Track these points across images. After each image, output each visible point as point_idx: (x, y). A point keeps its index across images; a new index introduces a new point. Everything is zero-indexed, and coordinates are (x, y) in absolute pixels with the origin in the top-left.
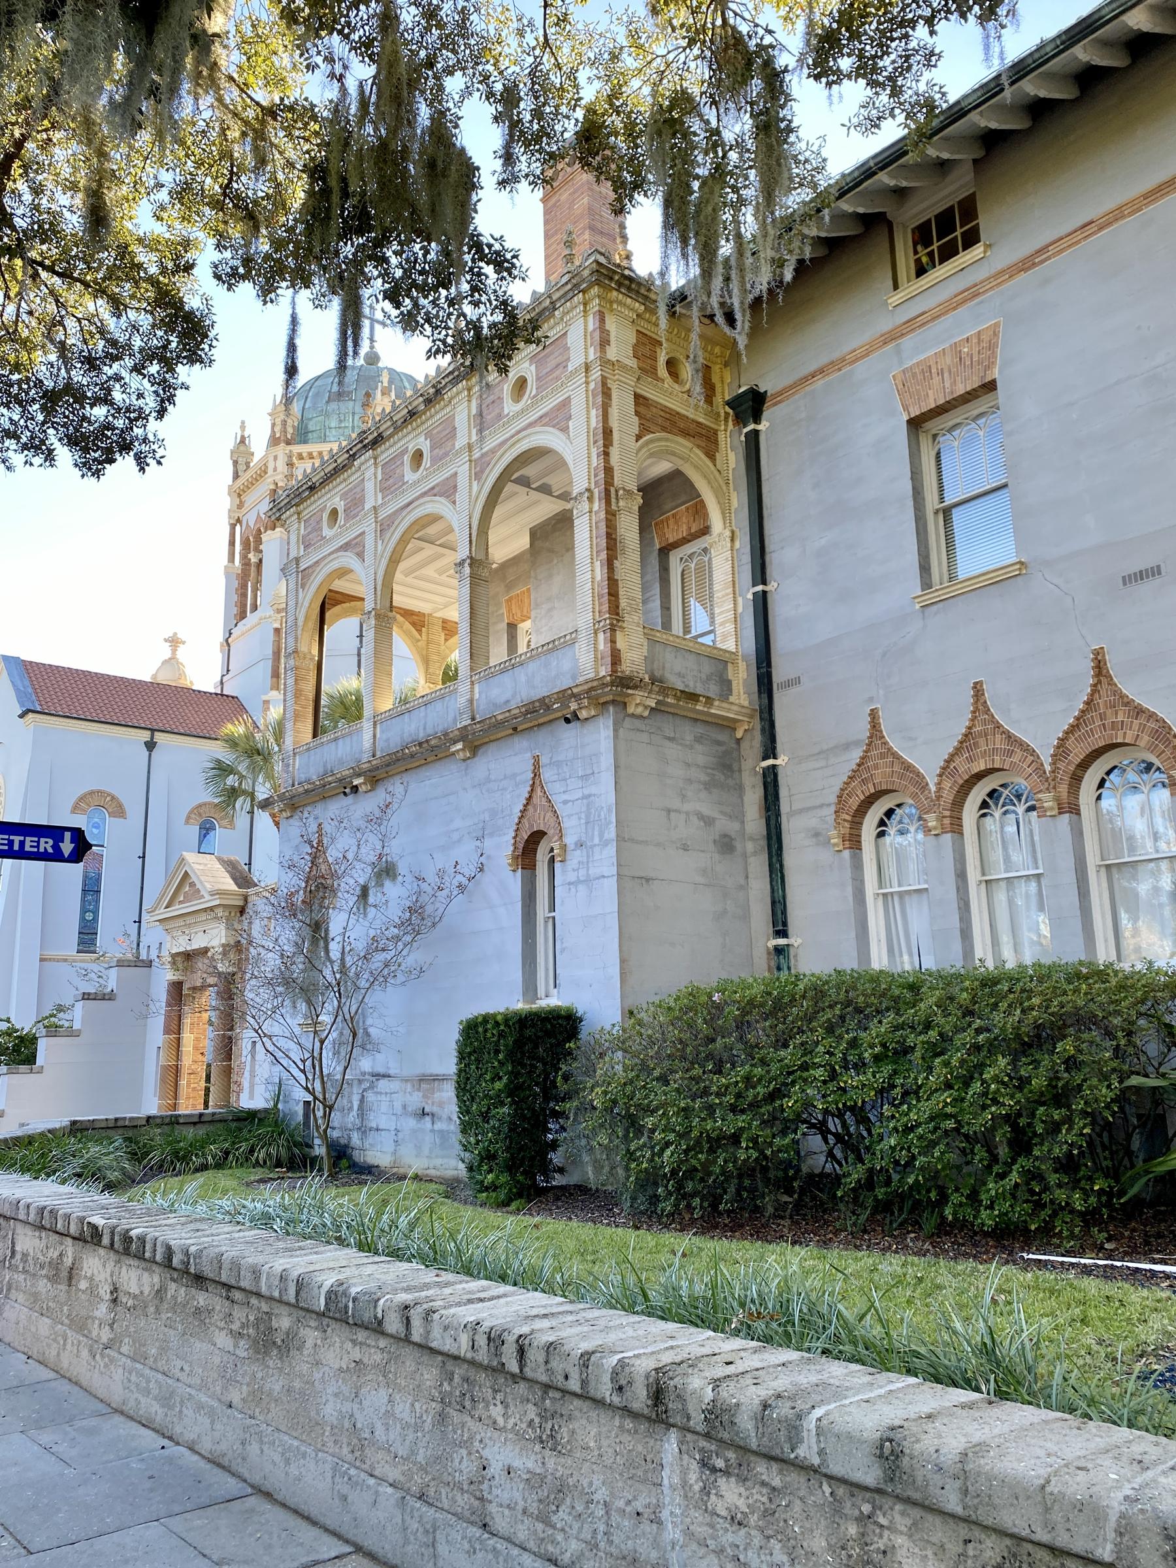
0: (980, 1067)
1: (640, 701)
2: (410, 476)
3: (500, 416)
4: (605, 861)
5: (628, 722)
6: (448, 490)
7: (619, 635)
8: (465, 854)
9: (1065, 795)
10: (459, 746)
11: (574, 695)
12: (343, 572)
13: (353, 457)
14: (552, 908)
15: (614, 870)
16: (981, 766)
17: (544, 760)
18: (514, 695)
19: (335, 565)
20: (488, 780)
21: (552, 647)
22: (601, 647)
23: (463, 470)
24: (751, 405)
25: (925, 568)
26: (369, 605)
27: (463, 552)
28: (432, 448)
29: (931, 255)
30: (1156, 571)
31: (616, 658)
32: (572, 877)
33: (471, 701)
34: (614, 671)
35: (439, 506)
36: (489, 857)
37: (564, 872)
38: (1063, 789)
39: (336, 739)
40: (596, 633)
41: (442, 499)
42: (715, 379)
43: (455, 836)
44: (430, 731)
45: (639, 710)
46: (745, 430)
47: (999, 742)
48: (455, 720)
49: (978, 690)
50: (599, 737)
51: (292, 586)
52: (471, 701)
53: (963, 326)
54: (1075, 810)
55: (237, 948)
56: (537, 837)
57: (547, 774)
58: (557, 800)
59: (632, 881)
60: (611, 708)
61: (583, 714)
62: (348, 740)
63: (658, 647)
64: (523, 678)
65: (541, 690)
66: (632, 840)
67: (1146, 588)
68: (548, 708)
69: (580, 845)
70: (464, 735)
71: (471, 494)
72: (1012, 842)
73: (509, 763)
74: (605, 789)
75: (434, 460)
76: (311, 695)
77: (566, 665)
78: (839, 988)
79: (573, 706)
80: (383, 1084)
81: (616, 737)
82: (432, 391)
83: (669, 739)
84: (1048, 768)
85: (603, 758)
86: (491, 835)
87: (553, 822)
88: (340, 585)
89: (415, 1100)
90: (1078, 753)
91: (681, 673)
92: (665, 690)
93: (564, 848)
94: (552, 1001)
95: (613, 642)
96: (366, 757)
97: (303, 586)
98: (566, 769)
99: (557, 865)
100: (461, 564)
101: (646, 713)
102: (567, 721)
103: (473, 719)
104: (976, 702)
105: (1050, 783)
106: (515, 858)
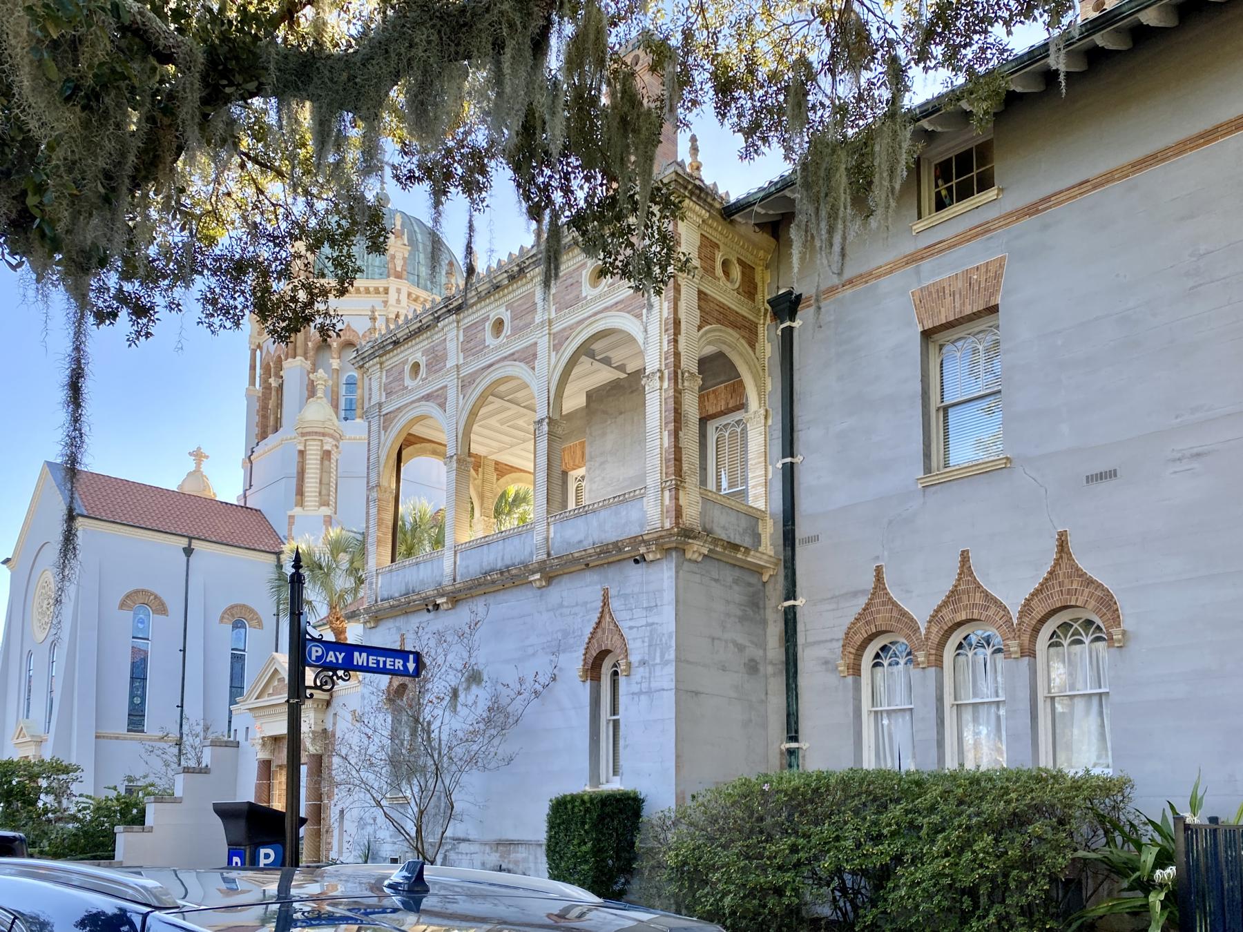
0: (968, 844)
1: (697, 548)
2: (490, 341)
3: (578, 298)
5: (686, 566)
6: (528, 357)
7: (681, 493)
8: (541, 665)
9: (1026, 643)
10: (537, 576)
11: (643, 541)
12: (420, 418)
13: (438, 319)
16: (963, 616)
17: (612, 592)
18: (586, 537)
20: (561, 606)
21: (622, 500)
22: (667, 502)
23: (543, 344)
24: (787, 306)
25: (927, 455)
27: (542, 412)
28: (513, 319)
33: (547, 539)
34: (677, 524)
35: (518, 370)
36: (561, 670)
38: (1026, 638)
40: (662, 490)
41: (522, 364)
42: (758, 279)
43: (530, 651)
44: (508, 562)
45: (696, 556)
46: (782, 326)
47: (978, 598)
48: (531, 554)
49: (965, 557)
50: (663, 577)
51: (374, 428)
52: (547, 539)
54: (1032, 654)
56: (604, 654)
57: (614, 604)
58: (624, 626)
60: (674, 554)
61: (650, 557)
64: (595, 523)
65: (611, 536)
68: (620, 550)
69: (643, 663)
70: (542, 568)
71: (549, 363)
72: (987, 677)
74: (667, 618)
75: (516, 330)
76: (390, 524)
77: (634, 515)
78: (861, 785)
79: (642, 550)
80: (463, 847)
81: (677, 577)
82: (516, 269)
84: (1015, 621)
85: (665, 594)
86: (564, 651)
87: (619, 643)
88: (418, 430)
89: (494, 858)
90: (1039, 610)
95: (677, 499)
96: (447, 581)
97: (385, 429)
98: (632, 601)
100: (540, 422)
102: (636, 561)
103: (549, 554)
104: (962, 566)
105: (1015, 632)
106: (585, 671)
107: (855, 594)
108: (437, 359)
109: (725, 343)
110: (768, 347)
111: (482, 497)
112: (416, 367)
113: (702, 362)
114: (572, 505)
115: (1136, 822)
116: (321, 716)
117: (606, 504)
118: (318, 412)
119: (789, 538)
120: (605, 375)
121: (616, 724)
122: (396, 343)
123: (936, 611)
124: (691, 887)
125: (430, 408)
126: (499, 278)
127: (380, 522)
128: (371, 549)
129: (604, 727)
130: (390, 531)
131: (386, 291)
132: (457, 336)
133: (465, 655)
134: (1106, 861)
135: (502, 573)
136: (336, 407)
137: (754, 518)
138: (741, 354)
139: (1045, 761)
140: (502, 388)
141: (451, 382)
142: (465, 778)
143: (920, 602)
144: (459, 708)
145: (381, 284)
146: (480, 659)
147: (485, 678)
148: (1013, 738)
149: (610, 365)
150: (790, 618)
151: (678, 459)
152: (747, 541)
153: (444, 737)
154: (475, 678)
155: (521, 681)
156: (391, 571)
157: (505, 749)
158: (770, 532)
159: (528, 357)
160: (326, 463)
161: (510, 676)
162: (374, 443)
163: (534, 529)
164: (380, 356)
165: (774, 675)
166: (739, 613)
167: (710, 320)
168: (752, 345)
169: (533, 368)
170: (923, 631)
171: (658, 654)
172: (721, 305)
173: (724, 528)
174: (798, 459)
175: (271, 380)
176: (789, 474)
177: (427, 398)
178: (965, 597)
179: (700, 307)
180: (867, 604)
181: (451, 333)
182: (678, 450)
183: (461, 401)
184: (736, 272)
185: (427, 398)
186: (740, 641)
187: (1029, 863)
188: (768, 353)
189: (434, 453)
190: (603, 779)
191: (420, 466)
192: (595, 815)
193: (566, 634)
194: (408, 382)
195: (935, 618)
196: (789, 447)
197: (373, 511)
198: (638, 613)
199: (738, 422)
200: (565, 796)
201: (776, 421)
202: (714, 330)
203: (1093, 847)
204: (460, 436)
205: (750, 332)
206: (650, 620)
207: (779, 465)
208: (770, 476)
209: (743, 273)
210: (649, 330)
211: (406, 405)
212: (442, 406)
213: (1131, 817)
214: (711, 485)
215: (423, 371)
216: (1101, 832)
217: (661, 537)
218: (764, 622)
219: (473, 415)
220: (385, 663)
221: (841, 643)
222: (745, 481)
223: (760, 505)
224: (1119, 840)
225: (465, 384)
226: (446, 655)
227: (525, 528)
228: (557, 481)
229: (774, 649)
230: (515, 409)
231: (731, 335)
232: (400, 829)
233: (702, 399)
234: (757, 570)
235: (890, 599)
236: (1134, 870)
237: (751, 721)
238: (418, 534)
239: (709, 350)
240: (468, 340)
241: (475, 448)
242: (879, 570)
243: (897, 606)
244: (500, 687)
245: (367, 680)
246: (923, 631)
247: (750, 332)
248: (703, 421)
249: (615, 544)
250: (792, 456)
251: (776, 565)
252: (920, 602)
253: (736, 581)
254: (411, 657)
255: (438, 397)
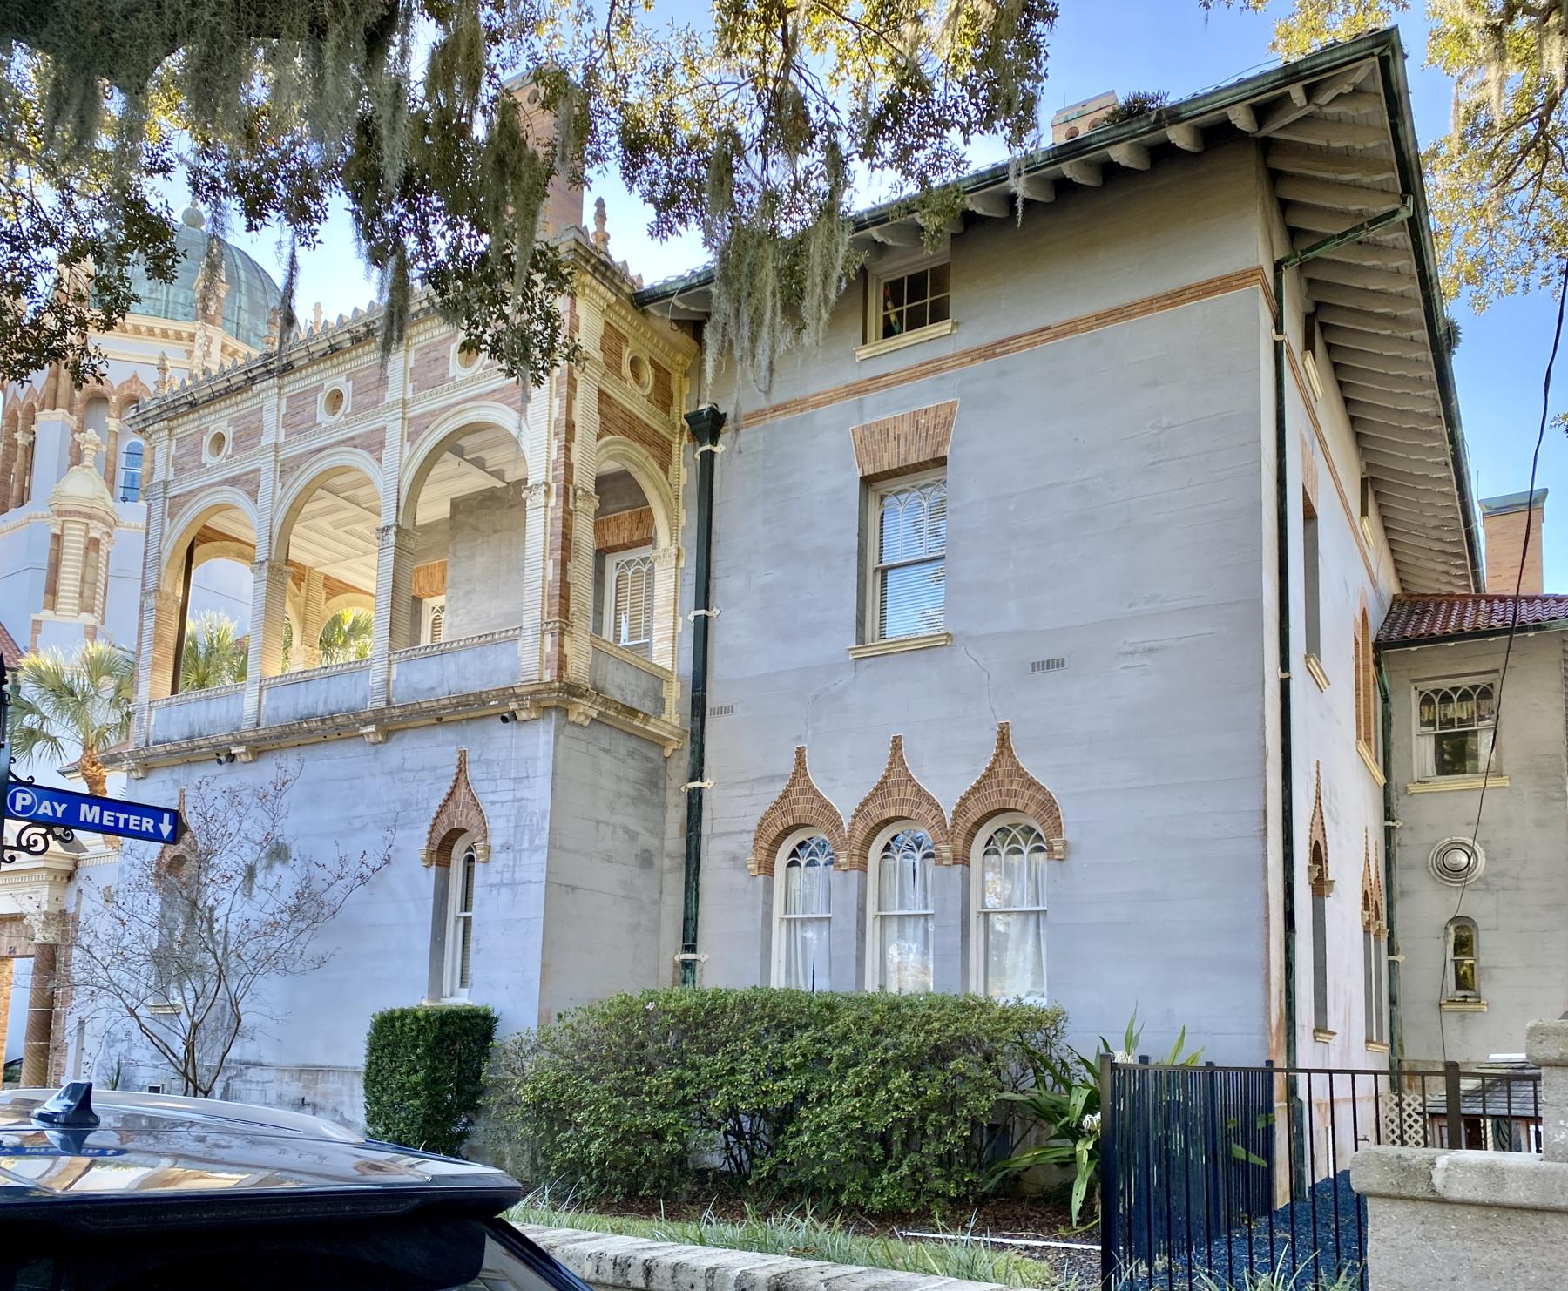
1: (584, 710)
4: (534, 866)
5: (569, 730)
7: (567, 639)
8: (372, 843)
10: (372, 728)
11: (515, 695)
14: (466, 906)
15: (543, 877)
17: (470, 756)
18: (441, 682)
19: (218, 499)
20: (402, 769)
21: (489, 641)
22: (548, 649)
26: (261, 554)
29: (899, 314)
30: (1059, 663)
31: (562, 664)
32: (495, 879)
33: (388, 681)
34: (560, 677)
36: (397, 850)
37: (486, 873)
39: (207, 699)
40: (543, 633)
43: (357, 824)
44: (333, 708)
48: (365, 699)
50: (538, 742)
52: (388, 681)
53: (924, 397)
55: (62, 918)
56: (456, 834)
57: (473, 771)
59: (559, 888)
61: (522, 715)
62: (223, 702)
63: (602, 657)
64: (453, 667)
65: (473, 686)
66: (562, 848)
67: (1049, 675)
68: (484, 704)
69: (506, 847)
70: (378, 718)
73: (430, 755)
77: (505, 661)
79: (513, 706)
80: (253, 1073)
81: (556, 744)
83: (606, 751)
85: (540, 764)
86: (403, 827)
87: (475, 821)
89: (294, 1090)
91: (622, 685)
92: (607, 702)
93: (488, 849)
94: (462, 999)
95: (561, 646)
98: (496, 769)
99: (478, 868)
101: (587, 723)
102: (505, 720)
103: (388, 702)
106: (430, 854)
107: (772, 779)
108: (248, 435)
109: (630, 460)
110: (684, 472)
111: (304, 621)
112: (219, 440)
113: (602, 481)
114: (426, 640)
115: (1068, 1061)
116: (58, 893)
117: (468, 645)
118: (84, 486)
119: (698, 707)
120: (476, 481)
121: (467, 922)
122: (192, 405)
123: (863, 805)
124: (550, 1128)
125: (237, 496)
126: (339, 339)
127: (158, 639)
128: (144, 675)
129: (451, 924)
130: (172, 652)
131: (192, 338)
132: (278, 406)
133: (268, 823)
134: (1033, 1104)
135: (323, 721)
136: (110, 481)
137: (658, 679)
138: (649, 477)
139: (976, 987)
140: (338, 481)
141: (267, 465)
142: (259, 983)
143: (845, 793)
144: (255, 891)
145: (186, 327)
146: (288, 829)
147: (294, 854)
148: (941, 958)
149: (483, 468)
150: (695, 803)
151: (564, 597)
152: (647, 706)
153: (232, 928)
154: (279, 853)
155: (343, 861)
156: (169, 705)
157: (314, 948)
158: (676, 696)
159: (374, 444)
160: (93, 555)
161: (329, 855)
162: (155, 534)
163: (371, 670)
164: (169, 419)
165: (672, 870)
166: (633, 793)
167: (613, 429)
168: (665, 468)
169: (379, 460)
170: (846, 827)
171: (526, 838)
172: (625, 411)
173: (620, 687)
174: (713, 613)
175: (18, 435)
176: (702, 629)
177: (233, 481)
178: (895, 791)
179: (600, 411)
180: (785, 792)
181: (269, 401)
182: (565, 586)
183: (279, 491)
184: (648, 374)
185: (233, 481)
186: (632, 827)
187: (949, 1104)
188: (683, 481)
189: (241, 556)
190: (446, 990)
191: (214, 570)
192: (431, 1036)
193: (407, 805)
194: (206, 457)
195: (860, 813)
196: (704, 597)
197: (149, 623)
198: (503, 784)
199: (645, 560)
200: (393, 1012)
201: (690, 564)
202: (618, 443)
203: (1021, 1088)
204: (275, 537)
205: (663, 453)
206: (519, 795)
207: (691, 618)
208: (679, 630)
209: (656, 377)
210: (537, 431)
211: (202, 489)
212: (253, 495)
213: (1063, 1055)
214: (608, 634)
215: (228, 446)
216: (1030, 1071)
217: (537, 692)
218: (663, 806)
219: (295, 510)
220: (127, 821)
221: (752, 836)
222: (649, 632)
223: (666, 663)
224: (1049, 1080)
225: (286, 470)
226: (240, 822)
227: (362, 665)
228: (406, 610)
229: (675, 841)
230: (352, 511)
231: (639, 452)
232: (164, 1050)
233: (598, 527)
234: (658, 743)
235: (812, 787)
236: (1063, 1115)
237: (639, 924)
238: (213, 659)
239: (611, 466)
240: (293, 411)
241: (294, 554)
242: (800, 752)
243: (819, 796)
244: (313, 868)
245: (125, 848)
246: (846, 827)
247: (663, 453)
248: (601, 554)
249: (478, 695)
250: (707, 608)
251: (682, 737)
252: (845, 793)
253: (631, 754)
254: (166, 816)
255: (248, 483)
